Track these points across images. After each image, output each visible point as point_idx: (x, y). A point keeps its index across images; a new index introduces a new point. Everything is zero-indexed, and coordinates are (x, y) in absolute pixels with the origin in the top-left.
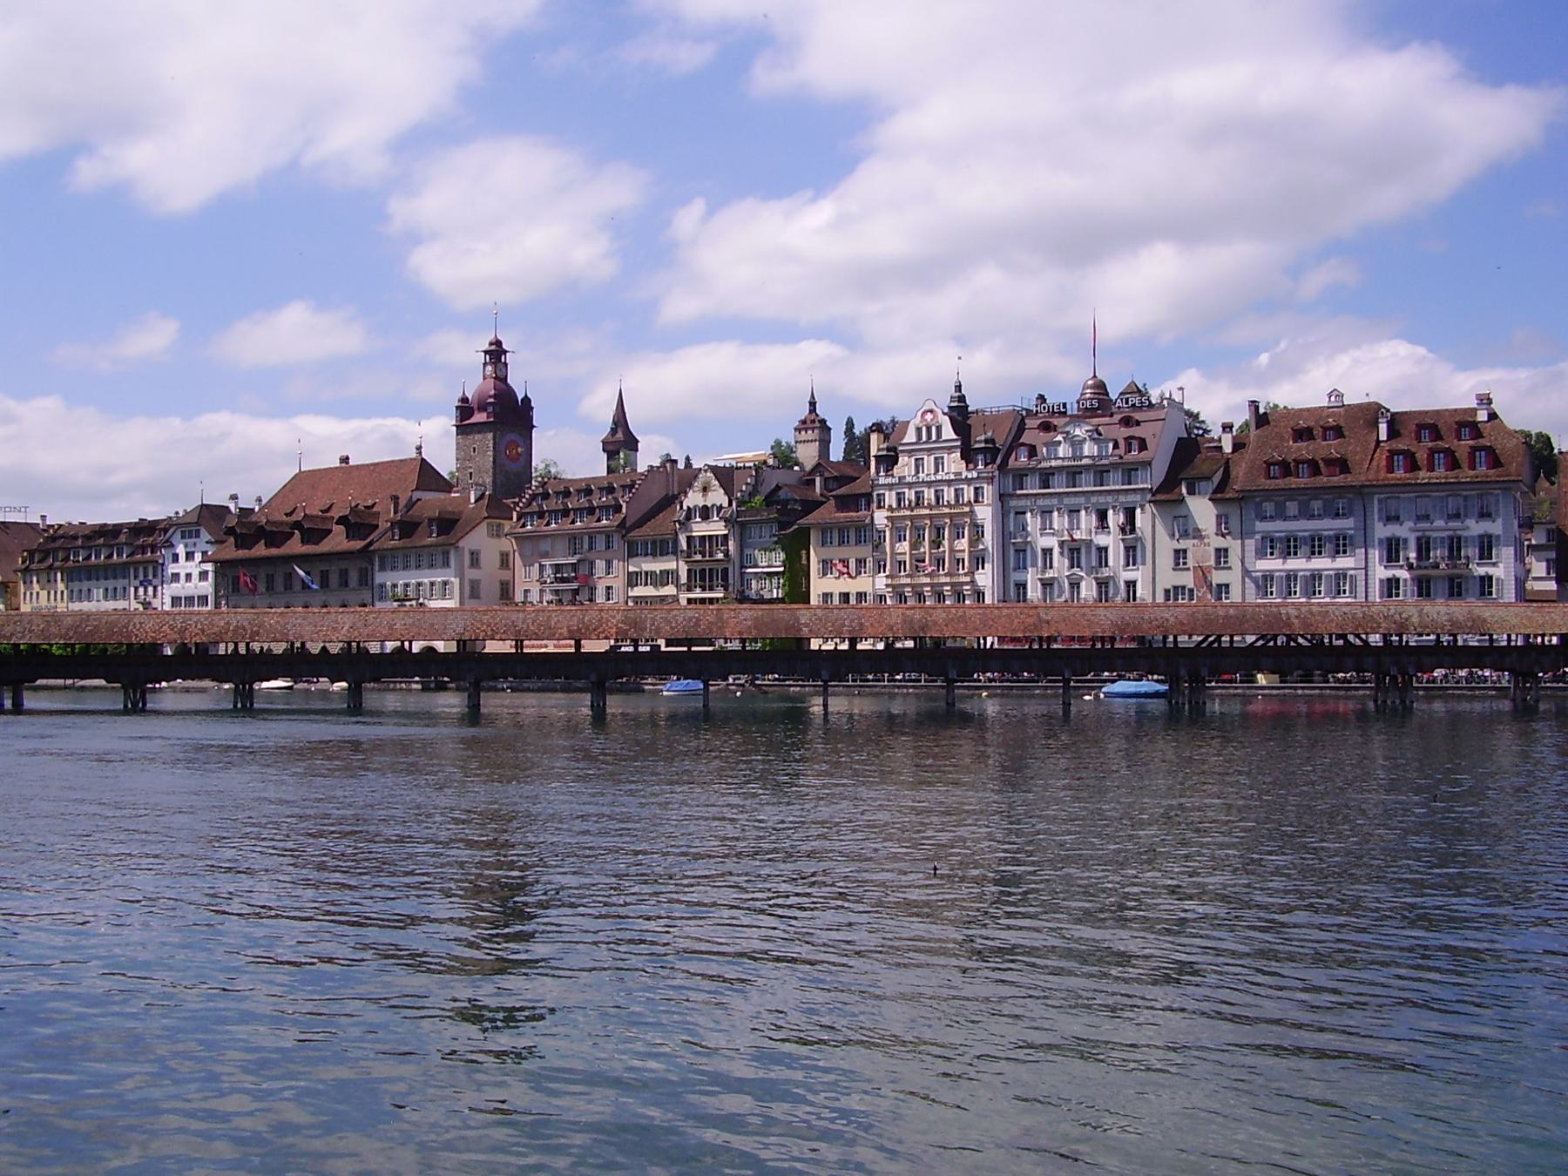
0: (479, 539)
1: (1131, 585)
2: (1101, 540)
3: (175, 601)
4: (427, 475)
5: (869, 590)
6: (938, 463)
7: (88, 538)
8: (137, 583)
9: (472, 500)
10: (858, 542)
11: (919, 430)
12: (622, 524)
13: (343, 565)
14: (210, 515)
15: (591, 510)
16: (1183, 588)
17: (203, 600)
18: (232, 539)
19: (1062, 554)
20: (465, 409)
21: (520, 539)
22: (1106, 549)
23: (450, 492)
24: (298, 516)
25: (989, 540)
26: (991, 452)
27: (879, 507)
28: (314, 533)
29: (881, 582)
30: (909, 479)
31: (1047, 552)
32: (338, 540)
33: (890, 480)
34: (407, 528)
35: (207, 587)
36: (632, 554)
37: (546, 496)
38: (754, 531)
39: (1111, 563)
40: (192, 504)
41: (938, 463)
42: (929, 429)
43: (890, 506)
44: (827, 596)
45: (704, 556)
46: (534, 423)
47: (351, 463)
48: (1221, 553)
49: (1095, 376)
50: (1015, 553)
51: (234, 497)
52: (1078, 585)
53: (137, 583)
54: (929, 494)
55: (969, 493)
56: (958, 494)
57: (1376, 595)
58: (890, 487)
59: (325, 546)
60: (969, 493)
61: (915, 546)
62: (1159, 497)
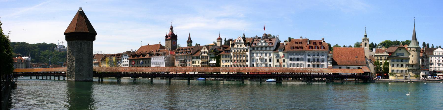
1: (270, 64)
2: (265, 58)
5: (230, 65)
6: (241, 45)
7: (110, 56)
8: (117, 63)
9: (168, 50)
10: (228, 57)
11: (238, 40)
12: (191, 54)
14: (128, 52)
15: (186, 52)
16: (278, 65)
17: (127, 65)
18: (132, 56)
19: (260, 60)
20: (167, 37)
22: (266, 59)
23: (165, 49)
24: (142, 53)
25: (248, 58)
26: (249, 44)
27: (231, 52)
28: (144, 55)
29: (232, 63)
30: (236, 48)
31: (257, 59)
33: (233, 48)
35: (128, 63)
39: (267, 61)
40: (125, 51)
41: (241, 45)
42: (239, 40)
43: (233, 52)
45: (204, 59)
46: (178, 39)
47: (150, 45)
48: (284, 60)
49: (265, 33)
50: (252, 59)
51: (132, 50)
52: (262, 64)
53: (117, 63)
54: (239, 50)
55: (245, 50)
56: (244, 50)
57: (307, 67)
58: (233, 49)
60: (245, 50)
61: (237, 58)
62: (274, 51)
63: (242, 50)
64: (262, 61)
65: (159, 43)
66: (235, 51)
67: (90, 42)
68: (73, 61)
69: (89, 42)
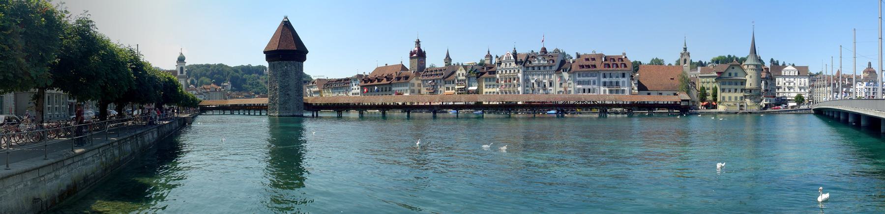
0: (413, 80)
2: (544, 81)
3: (353, 94)
4: (404, 68)
6: (510, 64)
10: (493, 81)
12: (443, 77)
13: (386, 86)
14: (360, 76)
15: (437, 75)
17: (358, 94)
20: (412, 54)
21: (423, 81)
24: (377, 76)
26: (521, 62)
29: (498, 90)
32: (385, 81)
34: (399, 78)
35: (359, 91)
36: (445, 84)
37: (428, 72)
38: (471, 79)
40: (356, 74)
41: (510, 64)
43: (500, 74)
44: (486, 92)
46: (426, 56)
51: (364, 73)
55: (516, 71)
56: (514, 71)
59: (382, 83)
60: (516, 71)
63: (512, 71)
64: (539, 86)
65: (400, 63)
66: (502, 71)
67: (299, 63)
68: (276, 90)
69: (297, 63)
